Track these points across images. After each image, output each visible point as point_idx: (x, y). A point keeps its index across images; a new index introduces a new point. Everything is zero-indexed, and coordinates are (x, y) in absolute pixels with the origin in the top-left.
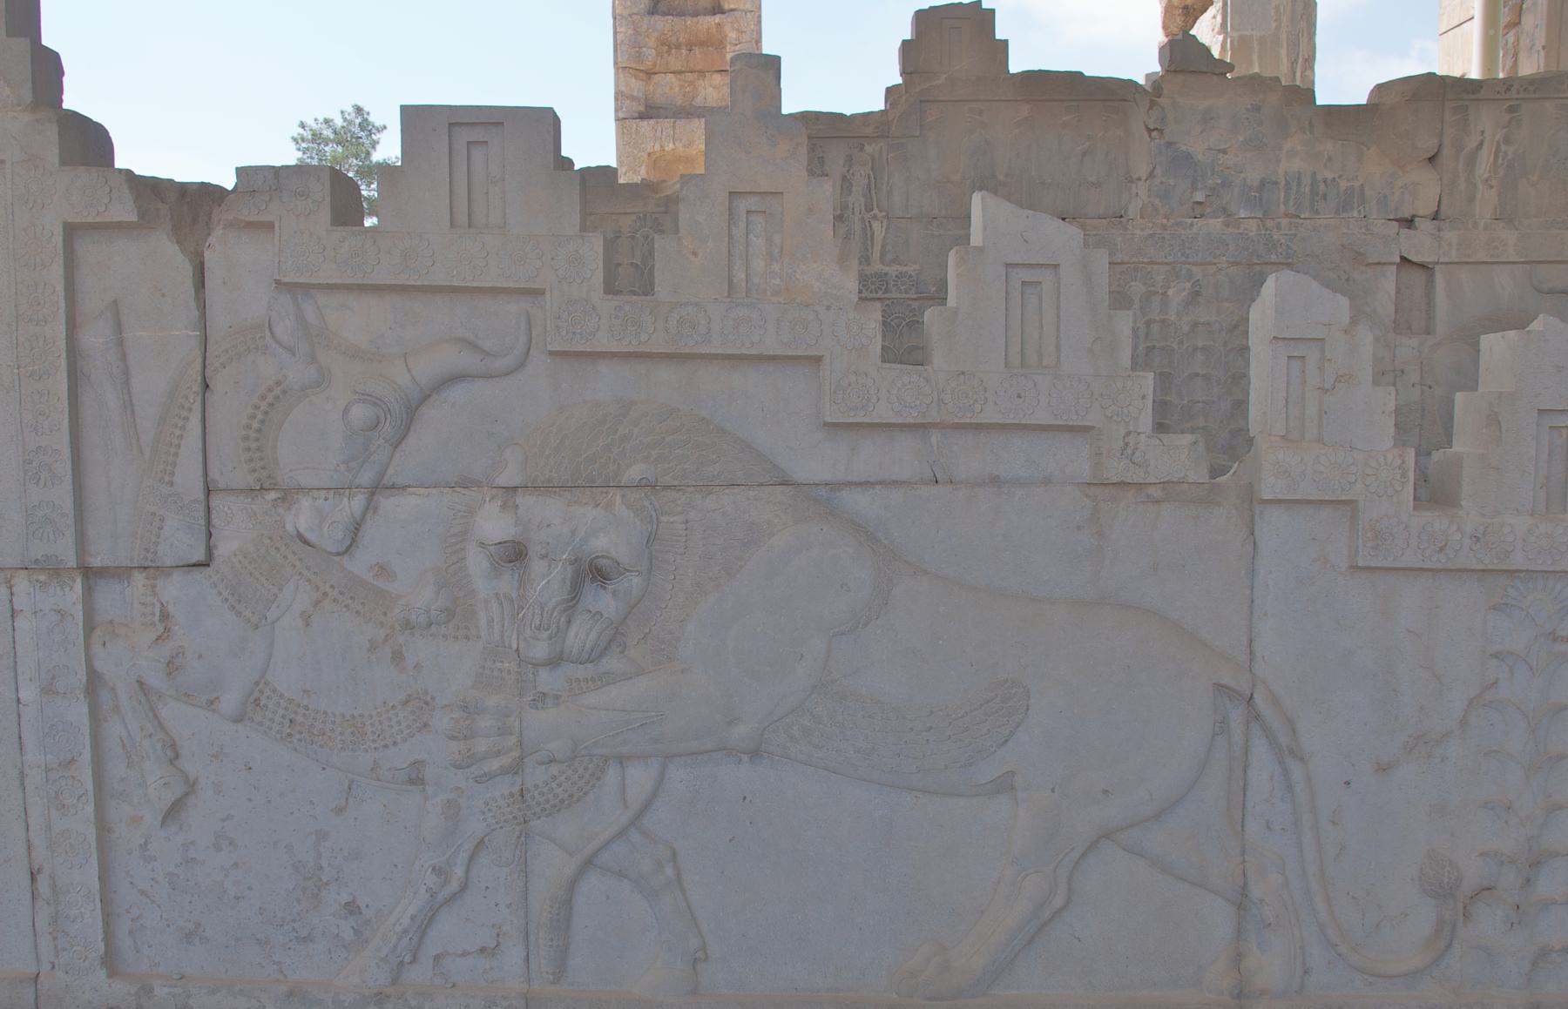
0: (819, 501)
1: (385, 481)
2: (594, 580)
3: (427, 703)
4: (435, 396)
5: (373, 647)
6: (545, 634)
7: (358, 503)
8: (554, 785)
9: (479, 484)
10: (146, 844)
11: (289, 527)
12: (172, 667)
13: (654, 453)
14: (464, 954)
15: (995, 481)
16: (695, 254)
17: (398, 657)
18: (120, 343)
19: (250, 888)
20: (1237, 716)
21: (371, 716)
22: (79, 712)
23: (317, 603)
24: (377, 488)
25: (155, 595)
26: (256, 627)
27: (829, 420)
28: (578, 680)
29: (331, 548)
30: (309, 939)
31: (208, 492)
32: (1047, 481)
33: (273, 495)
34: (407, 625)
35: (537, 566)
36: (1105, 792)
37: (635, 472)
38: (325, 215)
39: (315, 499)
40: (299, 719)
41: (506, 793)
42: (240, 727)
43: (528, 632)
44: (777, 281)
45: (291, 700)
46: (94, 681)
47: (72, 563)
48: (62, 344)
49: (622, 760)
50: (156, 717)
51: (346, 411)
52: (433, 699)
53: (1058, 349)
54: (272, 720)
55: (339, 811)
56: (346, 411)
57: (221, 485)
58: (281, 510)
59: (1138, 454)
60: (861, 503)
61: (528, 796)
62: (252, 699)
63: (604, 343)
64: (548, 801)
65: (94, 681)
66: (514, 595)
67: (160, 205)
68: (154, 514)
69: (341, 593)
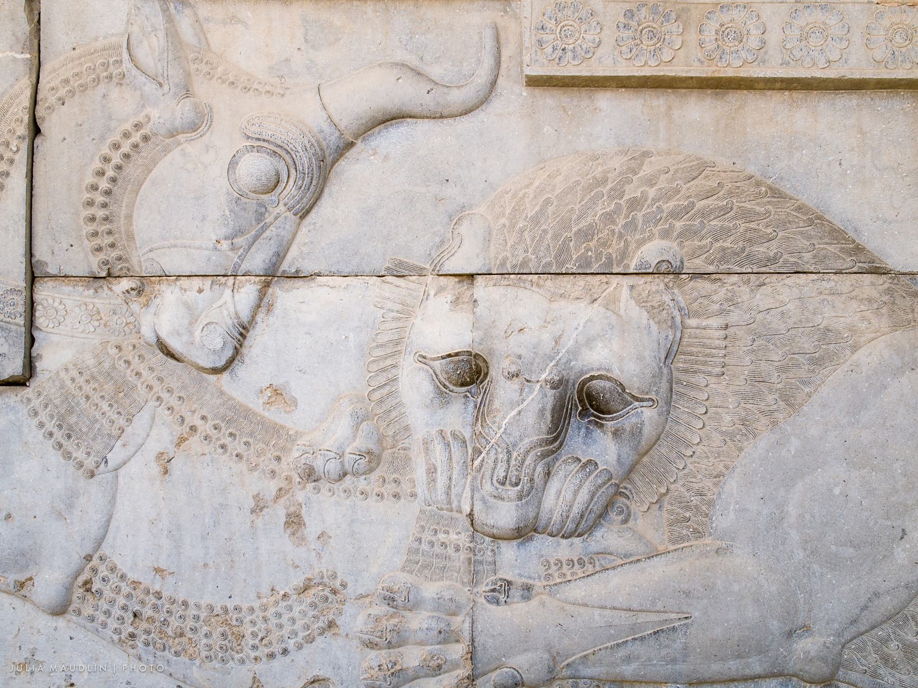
1: (285, 266)
2: (583, 415)
3: (334, 592)
4: (360, 145)
5: (259, 507)
6: (513, 492)
13: (679, 225)
17: (294, 522)
21: (252, 610)
23: (182, 440)
26: (92, 475)
28: (559, 563)
31: (33, 278)
33: (125, 284)
34: (310, 475)
35: (503, 391)
37: (651, 251)
40: (148, 612)
42: (61, 622)
45: (136, 584)
51: (233, 164)
52: (344, 586)
54: (108, 613)
56: (233, 164)
57: (52, 270)
62: (81, 579)
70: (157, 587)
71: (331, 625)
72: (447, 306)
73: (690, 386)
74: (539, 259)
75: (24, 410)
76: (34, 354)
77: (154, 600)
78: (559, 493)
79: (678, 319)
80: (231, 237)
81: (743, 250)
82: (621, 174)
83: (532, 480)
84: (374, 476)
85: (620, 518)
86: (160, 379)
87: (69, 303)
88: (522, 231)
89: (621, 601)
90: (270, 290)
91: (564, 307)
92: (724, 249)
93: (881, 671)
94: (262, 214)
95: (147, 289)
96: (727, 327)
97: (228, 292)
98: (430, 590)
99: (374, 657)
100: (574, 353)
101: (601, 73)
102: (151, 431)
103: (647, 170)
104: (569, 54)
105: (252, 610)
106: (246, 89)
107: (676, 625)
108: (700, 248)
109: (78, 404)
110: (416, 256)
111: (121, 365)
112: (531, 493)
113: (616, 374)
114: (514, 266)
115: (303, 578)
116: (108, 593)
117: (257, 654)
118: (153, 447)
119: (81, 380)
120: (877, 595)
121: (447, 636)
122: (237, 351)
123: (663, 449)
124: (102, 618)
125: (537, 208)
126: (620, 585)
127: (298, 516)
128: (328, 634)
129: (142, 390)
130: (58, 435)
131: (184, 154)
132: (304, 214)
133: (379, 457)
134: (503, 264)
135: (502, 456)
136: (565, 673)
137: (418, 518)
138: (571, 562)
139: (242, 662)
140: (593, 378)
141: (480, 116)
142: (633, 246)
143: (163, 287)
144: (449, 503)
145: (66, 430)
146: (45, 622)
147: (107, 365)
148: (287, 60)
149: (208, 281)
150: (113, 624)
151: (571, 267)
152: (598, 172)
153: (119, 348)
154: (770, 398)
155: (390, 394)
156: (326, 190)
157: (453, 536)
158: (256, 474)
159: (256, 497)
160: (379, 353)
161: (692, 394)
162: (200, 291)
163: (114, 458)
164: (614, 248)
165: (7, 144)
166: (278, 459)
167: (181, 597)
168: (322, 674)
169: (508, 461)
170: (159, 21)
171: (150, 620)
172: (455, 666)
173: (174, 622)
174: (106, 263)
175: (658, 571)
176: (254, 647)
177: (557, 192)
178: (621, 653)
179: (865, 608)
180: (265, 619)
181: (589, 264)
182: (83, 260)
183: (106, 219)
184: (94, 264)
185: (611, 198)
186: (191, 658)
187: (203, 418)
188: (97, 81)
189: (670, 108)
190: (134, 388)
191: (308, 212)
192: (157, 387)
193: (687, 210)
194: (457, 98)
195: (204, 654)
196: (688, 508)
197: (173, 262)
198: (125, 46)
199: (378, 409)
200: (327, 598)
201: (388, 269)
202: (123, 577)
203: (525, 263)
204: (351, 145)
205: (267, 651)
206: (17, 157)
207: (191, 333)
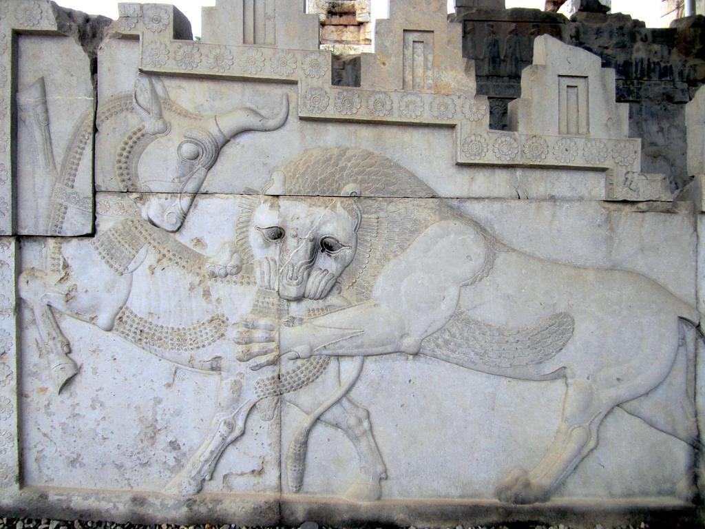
0: (451, 208)
1: (203, 190)
2: (322, 251)
3: (223, 322)
4: (232, 141)
5: (192, 288)
6: (295, 282)
7: (186, 201)
10: (49, 404)
11: (144, 216)
12: (68, 298)
13: (359, 177)
14: (242, 474)
15: (552, 198)
17: (207, 294)
18: (45, 103)
19: (112, 433)
21: (190, 329)
24: (195, 195)
25: (61, 253)
26: (122, 274)
27: (459, 161)
28: (313, 310)
30: (146, 464)
31: (95, 193)
32: (581, 199)
33: (135, 195)
34: (213, 275)
35: (291, 242)
36: (618, 379)
37: (349, 188)
38: (170, 32)
40: (146, 330)
41: (270, 377)
42: (110, 334)
43: (285, 281)
44: (431, 81)
45: (141, 319)
46: (20, 304)
47: (9, 232)
49: (338, 357)
50: (58, 327)
51: (180, 147)
52: (227, 319)
55: (169, 386)
56: (180, 147)
57: (103, 189)
59: (633, 184)
60: (476, 209)
61: (282, 379)
62: (118, 317)
64: (294, 382)
65: (20, 304)
66: (277, 259)
67: (72, 23)
68: (61, 205)
69: (174, 255)
70: (150, 320)
71: (222, 335)
72: (268, 208)
73: (366, 241)
74: (305, 190)
75: (92, 247)
76: (96, 224)
77: (149, 325)
78: (313, 283)
79: (359, 215)
81: (384, 188)
82: (338, 156)
83: (303, 278)
84: (239, 275)
85: (337, 292)
86: (150, 235)
87: (111, 203)
88: (298, 178)
89: (337, 325)
90: (196, 199)
91: (315, 210)
92: (377, 188)
93: (436, 350)
94: (192, 168)
95: (144, 197)
96: (378, 218)
97: (178, 200)
99: (240, 348)
100: (319, 228)
102: (147, 256)
103: (347, 155)
104: (317, 109)
106: (185, 116)
107: (359, 334)
108: (368, 187)
109: (115, 245)
111: (133, 229)
112: (302, 283)
113: (335, 236)
114: (295, 193)
115: (210, 316)
116: (129, 322)
117: (192, 347)
118: (147, 263)
119: (116, 235)
120: (434, 321)
122: (182, 223)
123: (354, 265)
124: (128, 332)
125: (304, 169)
127: (209, 291)
128: (221, 339)
129: (142, 239)
130: (107, 257)
132: (210, 168)
133: (241, 268)
134: (291, 191)
135: (291, 269)
136: (316, 353)
137: (257, 293)
139: (186, 350)
140: (326, 238)
141: (281, 131)
142: (342, 185)
143: (151, 197)
144: (270, 286)
145: (111, 255)
147: (127, 229)
148: (202, 105)
149: (170, 195)
150: (131, 334)
152: (328, 155)
153: (133, 221)
154: (395, 246)
155: (245, 242)
156: (218, 160)
157: (271, 300)
158: (190, 274)
159: (191, 284)
160: (241, 225)
161: (365, 244)
163: (131, 267)
164: (335, 186)
165: (84, 136)
166: (200, 268)
167: (160, 324)
168: (219, 355)
169: (293, 270)
170: (148, 87)
171: (148, 333)
172: (272, 351)
173: (158, 334)
174: (127, 187)
175: (351, 313)
176: (191, 344)
177: (312, 163)
178: (338, 345)
179: (430, 326)
180: (196, 333)
181: (325, 193)
184: (122, 187)
185: (333, 166)
186: (165, 349)
187: (169, 251)
188: (122, 110)
189: (356, 130)
190: (139, 238)
191: (211, 167)
192: (149, 238)
193: (362, 172)
194: (271, 123)
196: (364, 288)
197: (155, 187)
198: (134, 96)
199: (240, 248)
200: (220, 325)
201: (244, 192)
202: (136, 316)
203: (299, 191)
204: (229, 141)
205: (197, 346)
206: (88, 141)
207: (163, 216)
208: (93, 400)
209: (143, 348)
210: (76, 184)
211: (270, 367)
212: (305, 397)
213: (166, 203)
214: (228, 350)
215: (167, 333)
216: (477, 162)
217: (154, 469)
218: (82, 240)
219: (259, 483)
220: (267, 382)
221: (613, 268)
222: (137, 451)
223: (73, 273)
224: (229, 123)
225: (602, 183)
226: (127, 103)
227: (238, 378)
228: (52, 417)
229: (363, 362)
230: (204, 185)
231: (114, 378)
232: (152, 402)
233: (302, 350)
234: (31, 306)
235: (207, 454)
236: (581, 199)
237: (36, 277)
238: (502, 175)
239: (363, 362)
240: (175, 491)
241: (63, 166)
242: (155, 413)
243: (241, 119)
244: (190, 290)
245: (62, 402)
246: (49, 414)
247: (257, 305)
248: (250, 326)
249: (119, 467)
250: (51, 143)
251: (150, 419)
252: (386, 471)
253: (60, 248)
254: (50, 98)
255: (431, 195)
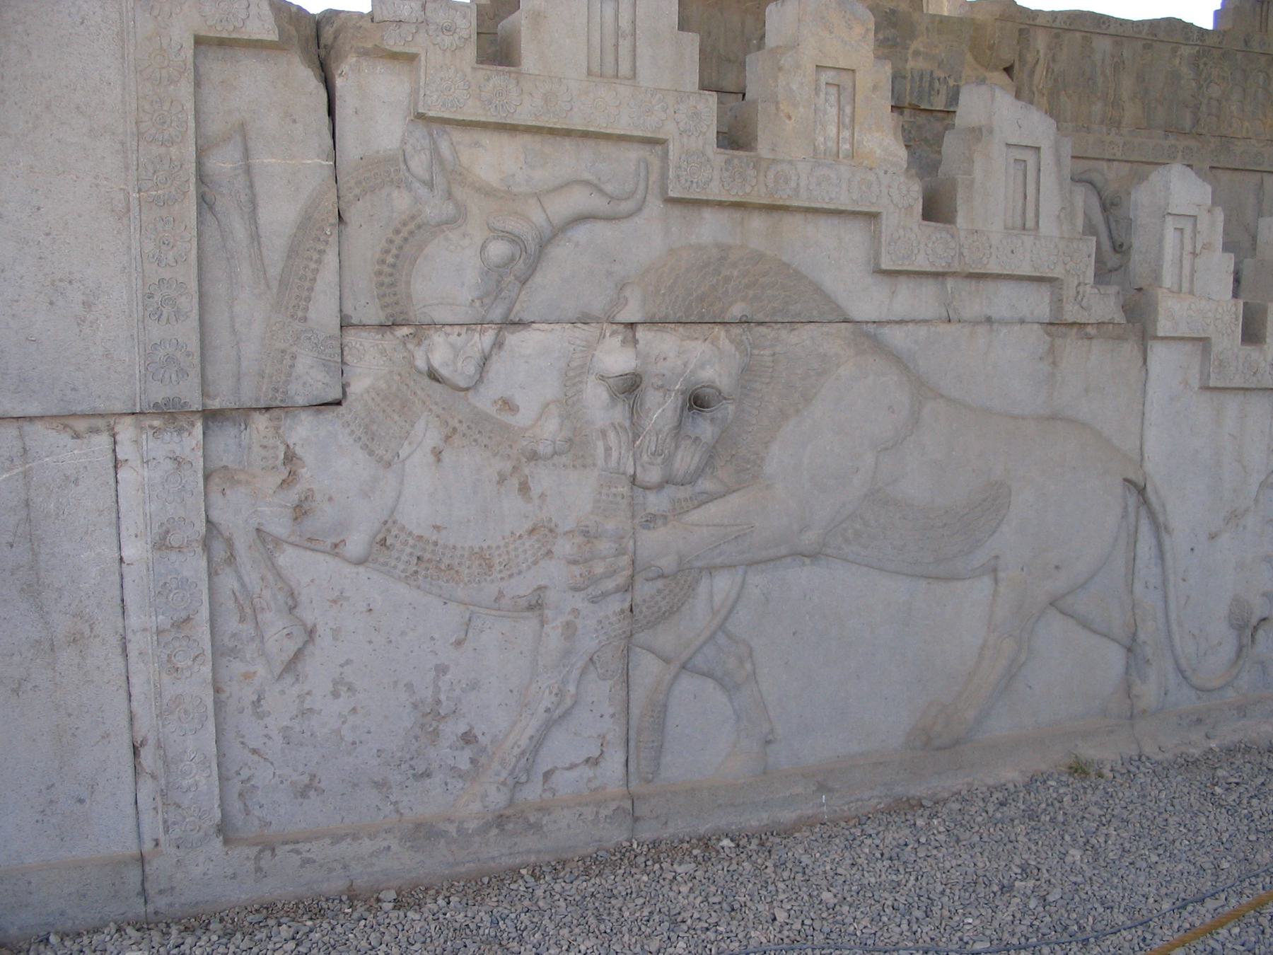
0: (867, 337)
1: (512, 317)
3: (551, 531)
5: (502, 479)
6: (659, 460)
7: (489, 336)
8: (659, 598)
9: (598, 320)
10: (259, 700)
11: (421, 364)
12: (301, 511)
13: (751, 293)
14: (572, 767)
15: (989, 320)
16: (790, 118)
17: (524, 488)
18: (248, 170)
20: (1133, 500)
22: (194, 565)
26: (389, 464)
29: (463, 384)
30: (427, 774)
32: (1022, 321)
33: (405, 331)
34: (534, 456)
35: (652, 398)
36: (1057, 567)
37: (737, 310)
38: (471, 52)
39: (447, 335)
40: (427, 556)
42: (361, 569)
43: (645, 458)
45: (420, 538)
48: (191, 168)
49: (711, 570)
51: (483, 247)
53: (1037, 215)
54: (398, 559)
55: (459, 643)
56: (483, 247)
57: (354, 321)
58: (410, 346)
60: (897, 337)
61: (636, 611)
63: (715, 192)
66: (627, 424)
70: (434, 538)
80: (480, 298)
91: (690, 344)
97: (477, 336)
98: (610, 525)
99: (576, 570)
100: (693, 372)
101: (711, 198)
105: (498, 547)
110: (597, 307)
113: (718, 383)
116: (398, 545)
121: (620, 552)
126: (713, 510)
130: (364, 439)
131: (447, 239)
138: (686, 500)
139: (492, 581)
141: (637, 220)
143: (432, 332)
146: (348, 570)
149: (465, 328)
151: (693, 319)
157: (620, 489)
159: (499, 473)
160: (571, 374)
162: (459, 335)
166: (511, 447)
168: (542, 583)
170: (426, 142)
171: (429, 561)
173: (446, 561)
174: (392, 316)
175: (735, 500)
176: (501, 571)
182: (373, 314)
183: (392, 285)
184: (381, 317)
186: (457, 583)
187: (460, 422)
194: (626, 206)
195: (466, 579)
197: (441, 315)
198: (401, 159)
202: (410, 534)
208: (336, 683)
209: (419, 587)
210: (312, 314)
211: (618, 596)
212: (665, 638)
213: (459, 341)
214: (555, 573)
215: (462, 556)
216: (905, 268)
217: (438, 779)
218: (320, 412)
219: (595, 777)
220: (614, 619)
221: (1053, 417)
222: (408, 756)
223: (304, 470)
224: (562, 207)
225: (1047, 300)
226: (387, 171)
227: (571, 618)
228: (267, 720)
229: (746, 573)
230: (515, 310)
231: (370, 642)
232: (433, 673)
233: (667, 563)
234: (227, 534)
235: (524, 742)
236: (1022, 321)
237: (239, 482)
238: (929, 289)
239: (746, 573)
240: (476, 807)
241: (283, 283)
242: (437, 689)
243: (579, 200)
244: (498, 483)
245: (283, 692)
246: (260, 716)
247: (598, 501)
248: (588, 535)
249: (382, 785)
250: (259, 243)
251: (430, 700)
252: (772, 731)
253: (277, 428)
254: (255, 161)
255: (842, 318)
